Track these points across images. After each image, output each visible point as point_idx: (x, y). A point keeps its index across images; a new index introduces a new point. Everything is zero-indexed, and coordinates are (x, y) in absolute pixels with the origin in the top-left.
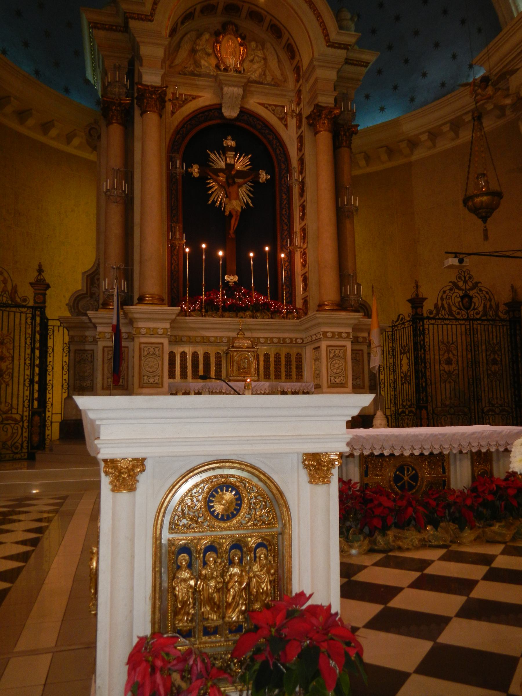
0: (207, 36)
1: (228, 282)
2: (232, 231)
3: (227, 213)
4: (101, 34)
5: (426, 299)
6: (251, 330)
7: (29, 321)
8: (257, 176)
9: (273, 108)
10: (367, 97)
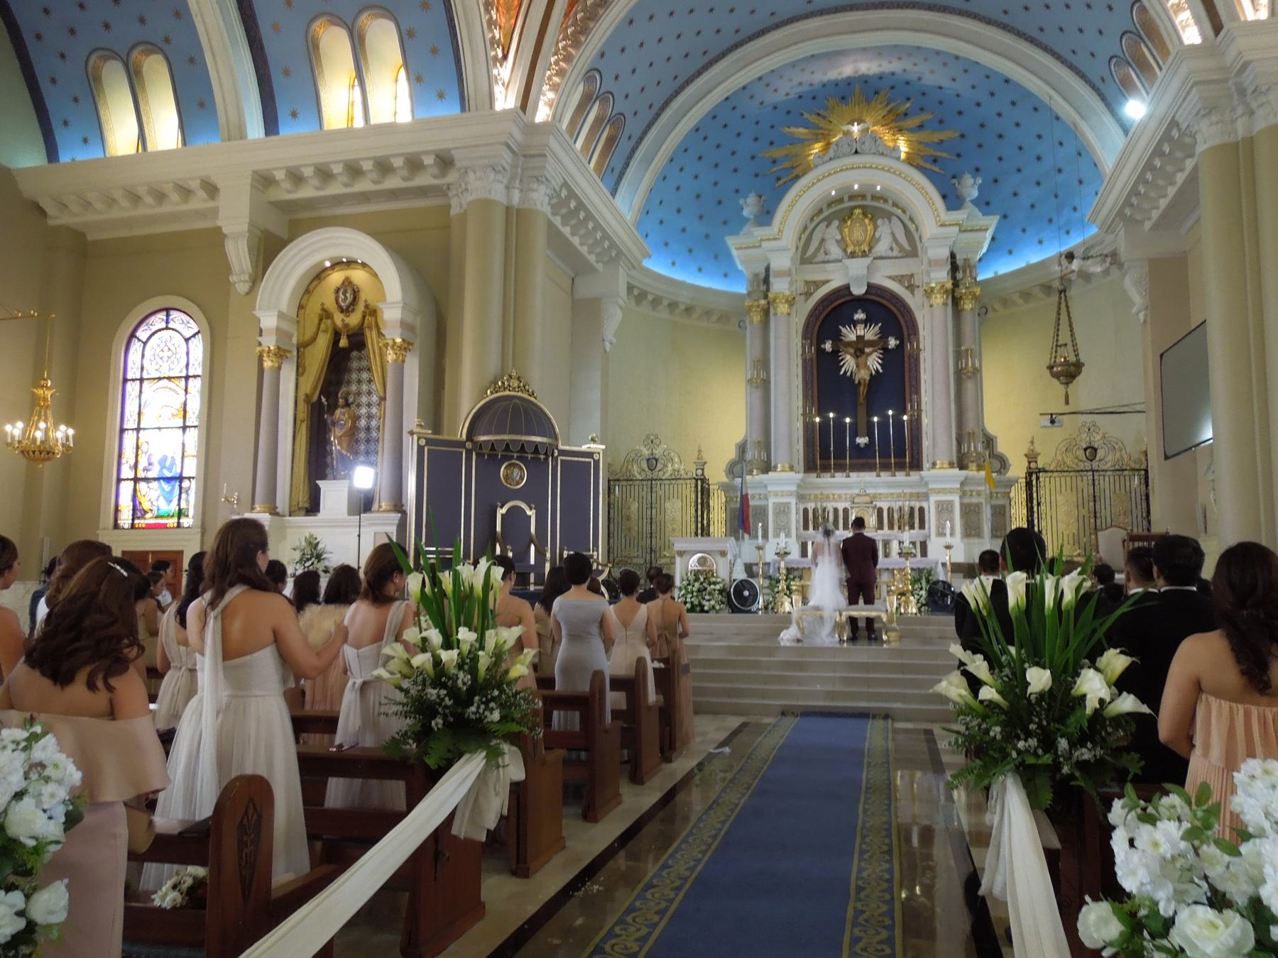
0: (836, 223)
1: (859, 444)
2: (861, 399)
3: (857, 382)
4: (741, 252)
5: (1039, 454)
6: (875, 487)
7: (693, 489)
8: (887, 343)
9: (899, 279)
10: (1024, 230)
